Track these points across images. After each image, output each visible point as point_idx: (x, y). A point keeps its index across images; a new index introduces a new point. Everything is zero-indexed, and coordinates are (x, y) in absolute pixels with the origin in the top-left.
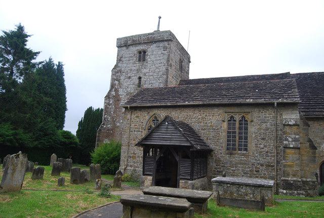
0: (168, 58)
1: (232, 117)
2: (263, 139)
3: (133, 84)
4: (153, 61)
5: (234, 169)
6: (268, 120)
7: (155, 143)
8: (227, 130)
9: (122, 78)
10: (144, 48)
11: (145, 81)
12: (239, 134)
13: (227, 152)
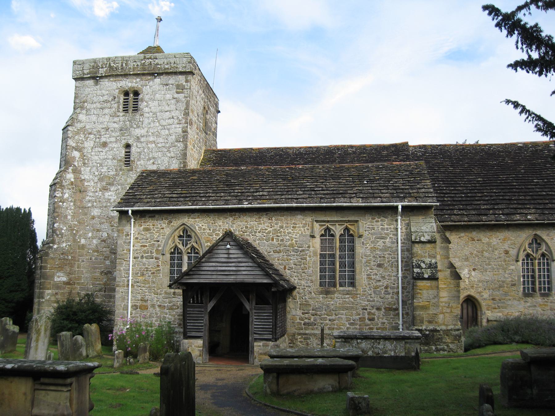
0: (187, 108)
1: (328, 229)
2: (380, 266)
3: (114, 159)
4: (155, 113)
5: (333, 317)
6: (387, 234)
8: (319, 252)
10: (134, 85)
12: (340, 258)
13: (320, 289)
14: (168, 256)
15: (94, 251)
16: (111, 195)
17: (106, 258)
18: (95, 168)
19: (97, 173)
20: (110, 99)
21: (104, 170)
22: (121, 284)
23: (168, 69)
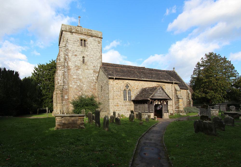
3: (79, 60)
7: (156, 98)
9: (69, 54)
10: (84, 38)
11: (88, 60)
14: (123, 91)
15: (75, 89)
16: (80, 72)
17: (80, 91)
18: (73, 63)
19: (74, 64)
20: (77, 41)
21: (76, 64)
22: (111, 99)
23: (96, 35)
